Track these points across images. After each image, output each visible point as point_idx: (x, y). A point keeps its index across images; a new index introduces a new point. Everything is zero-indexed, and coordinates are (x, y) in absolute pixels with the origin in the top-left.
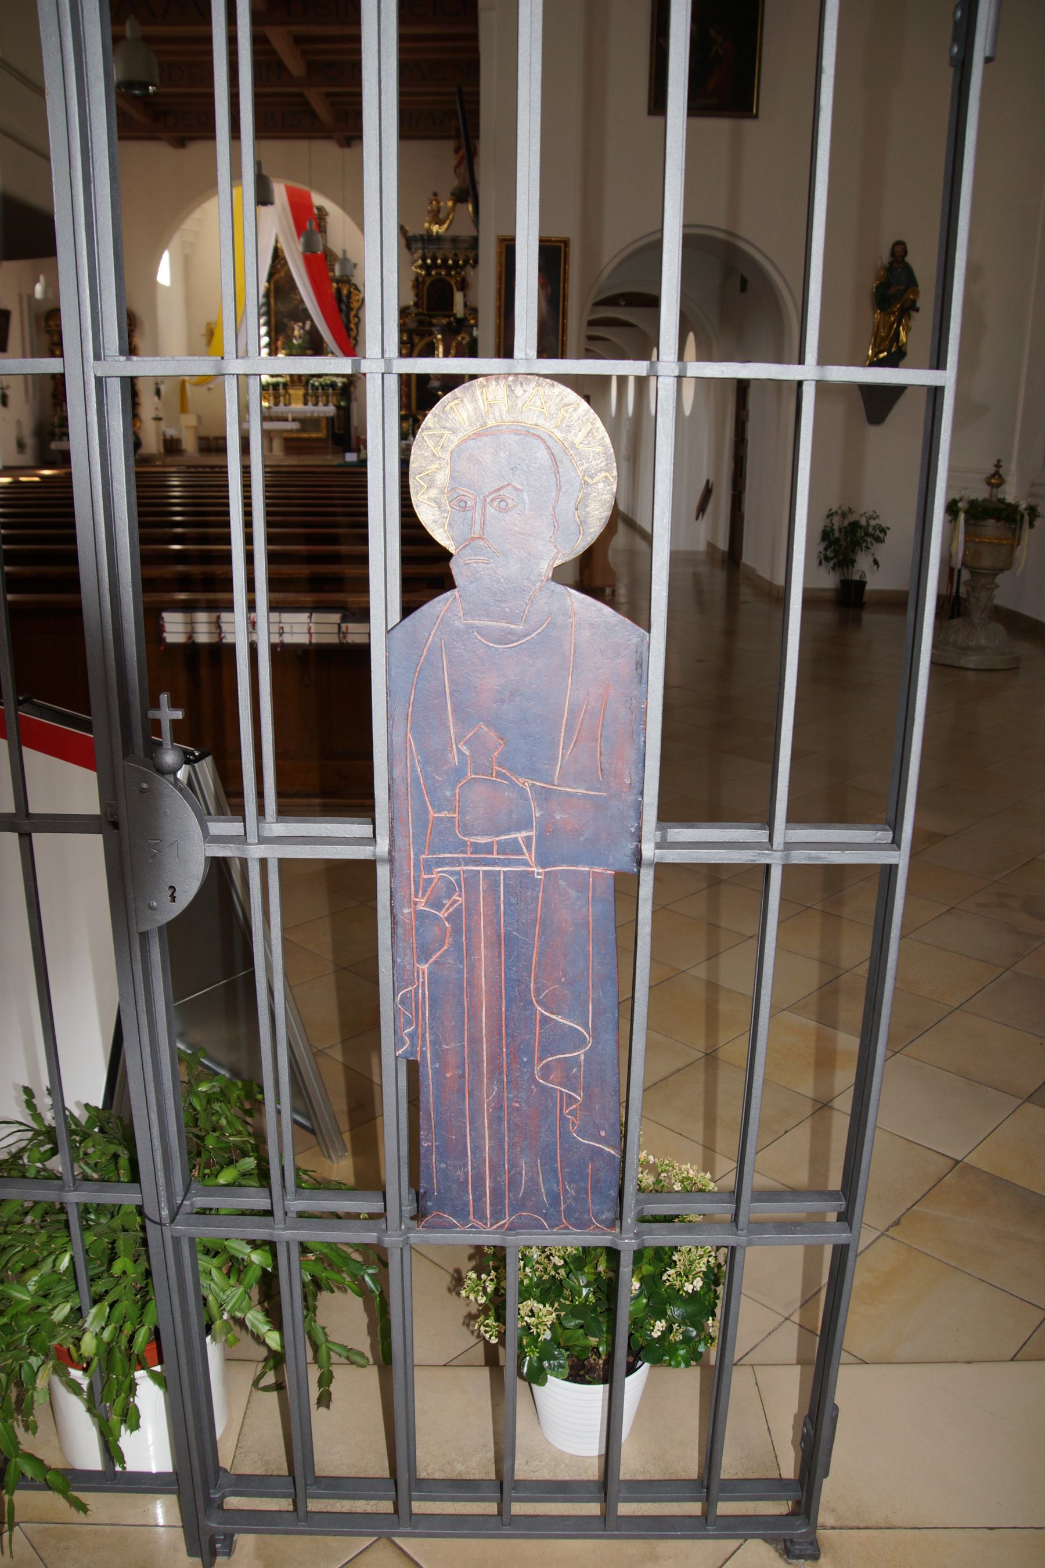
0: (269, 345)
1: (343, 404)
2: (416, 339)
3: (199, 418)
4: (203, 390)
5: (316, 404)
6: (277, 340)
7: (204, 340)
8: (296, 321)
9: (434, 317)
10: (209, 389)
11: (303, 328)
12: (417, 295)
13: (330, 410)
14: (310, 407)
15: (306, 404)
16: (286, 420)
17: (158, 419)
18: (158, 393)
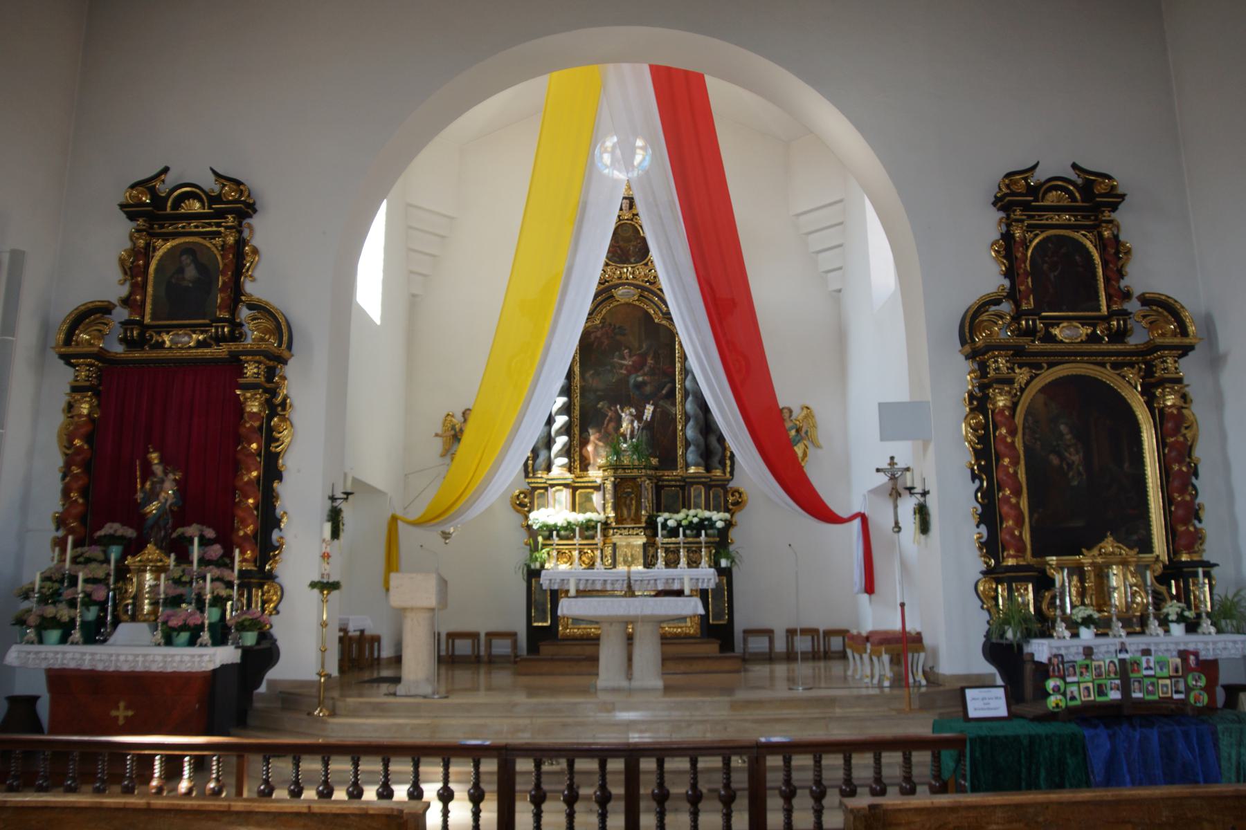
0: (567, 451)
1: (724, 563)
2: (1022, 375)
3: (443, 584)
4: (431, 537)
5: (672, 563)
6: (584, 442)
7: (438, 445)
8: (626, 402)
9: (1056, 322)
10: (446, 536)
11: (639, 416)
12: (1009, 274)
13: (706, 575)
14: (660, 569)
15: (648, 564)
16: (679, 593)
17: (326, 586)
18: (335, 517)
